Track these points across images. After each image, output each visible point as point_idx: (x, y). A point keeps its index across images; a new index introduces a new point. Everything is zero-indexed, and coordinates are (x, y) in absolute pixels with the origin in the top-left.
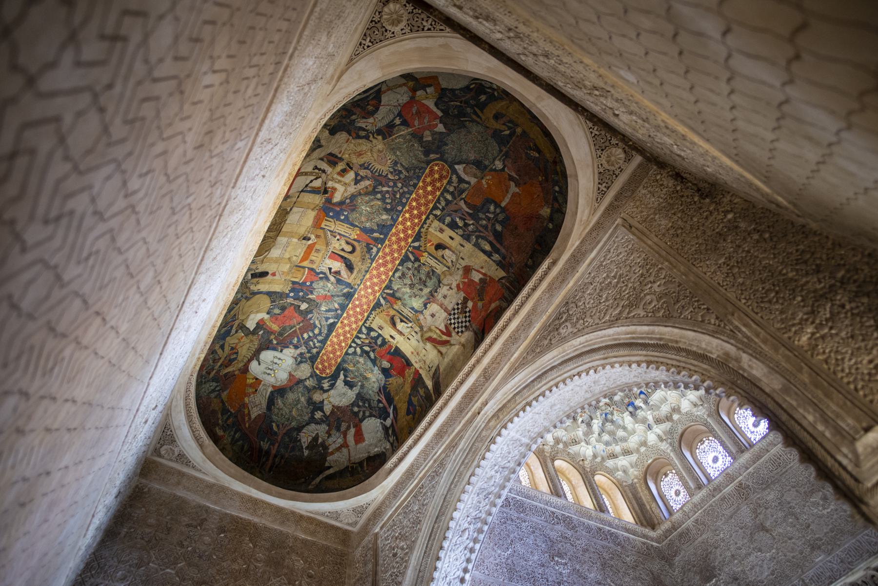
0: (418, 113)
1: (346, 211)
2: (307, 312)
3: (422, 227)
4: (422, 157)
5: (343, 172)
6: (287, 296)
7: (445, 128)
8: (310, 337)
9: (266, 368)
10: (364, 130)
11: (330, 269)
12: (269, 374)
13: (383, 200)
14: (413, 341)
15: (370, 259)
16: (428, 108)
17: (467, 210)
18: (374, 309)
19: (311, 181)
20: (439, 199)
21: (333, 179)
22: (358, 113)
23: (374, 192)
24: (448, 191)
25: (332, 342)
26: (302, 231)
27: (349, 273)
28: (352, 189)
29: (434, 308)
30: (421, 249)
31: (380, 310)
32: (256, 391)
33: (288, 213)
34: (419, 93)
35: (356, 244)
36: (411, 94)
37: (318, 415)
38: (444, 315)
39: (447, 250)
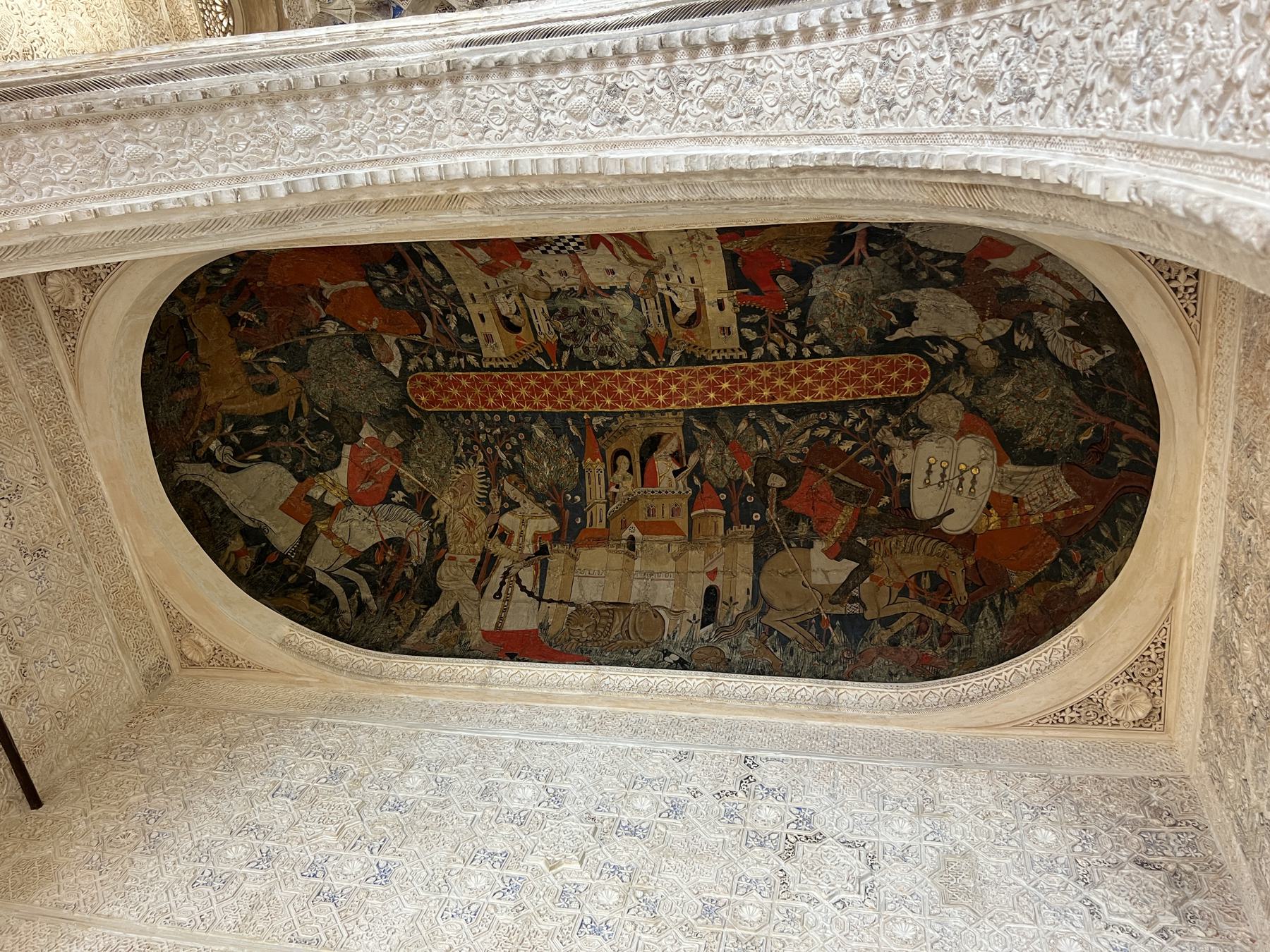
0: (368, 477)
1: (565, 498)
2: (787, 470)
3: (510, 369)
4: (425, 427)
5: (505, 537)
6: (763, 522)
7: (361, 427)
8: (844, 438)
9: (959, 493)
10: (431, 540)
11: (676, 473)
12: (974, 481)
13: (517, 450)
14: (688, 271)
15: (615, 420)
16: (350, 472)
17: (428, 321)
18: (704, 361)
19: (523, 589)
20: (455, 370)
21: (521, 548)
22: (401, 571)
23: (516, 470)
24: (435, 363)
25: (830, 393)
26: (617, 560)
27: (665, 438)
28: (528, 506)
29: (597, 278)
30: (541, 351)
31: (696, 351)
32: (1015, 500)
33: (578, 607)
34: (332, 501)
35: (609, 457)
36: (341, 512)
37: (1024, 342)
38: (585, 260)
39: (504, 313)
